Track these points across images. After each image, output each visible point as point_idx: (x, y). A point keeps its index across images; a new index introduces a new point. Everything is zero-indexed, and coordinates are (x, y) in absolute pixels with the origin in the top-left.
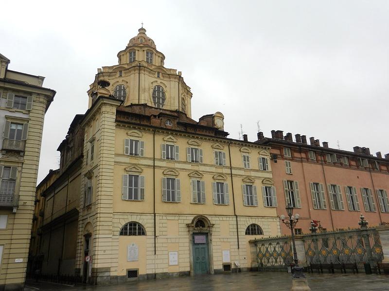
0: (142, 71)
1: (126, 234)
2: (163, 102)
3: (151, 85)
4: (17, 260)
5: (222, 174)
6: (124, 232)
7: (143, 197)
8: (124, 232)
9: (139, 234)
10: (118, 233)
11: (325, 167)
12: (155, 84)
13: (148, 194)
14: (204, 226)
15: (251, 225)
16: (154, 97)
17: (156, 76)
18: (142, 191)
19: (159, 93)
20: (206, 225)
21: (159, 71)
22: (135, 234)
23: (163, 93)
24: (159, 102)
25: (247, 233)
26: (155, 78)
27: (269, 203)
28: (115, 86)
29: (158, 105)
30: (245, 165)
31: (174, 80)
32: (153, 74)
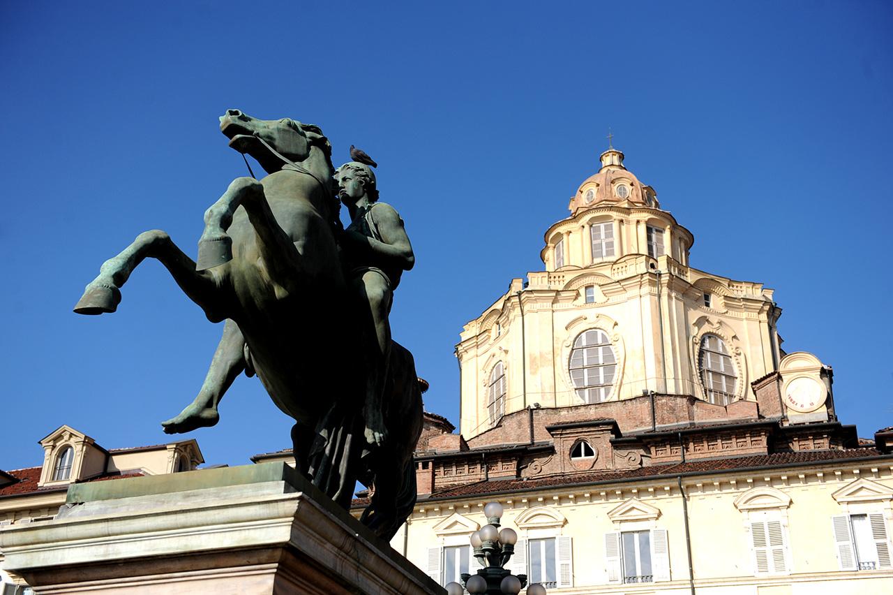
2: (609, 377)
12: (574, 331)
17: (582, 300)
19: (590, 357)
21: (588, 281)
23: (606, 345)
24: (594, 387)
26: (579, 307)
30: (762, 563)
31: (635, 291)
32: (567, 299)
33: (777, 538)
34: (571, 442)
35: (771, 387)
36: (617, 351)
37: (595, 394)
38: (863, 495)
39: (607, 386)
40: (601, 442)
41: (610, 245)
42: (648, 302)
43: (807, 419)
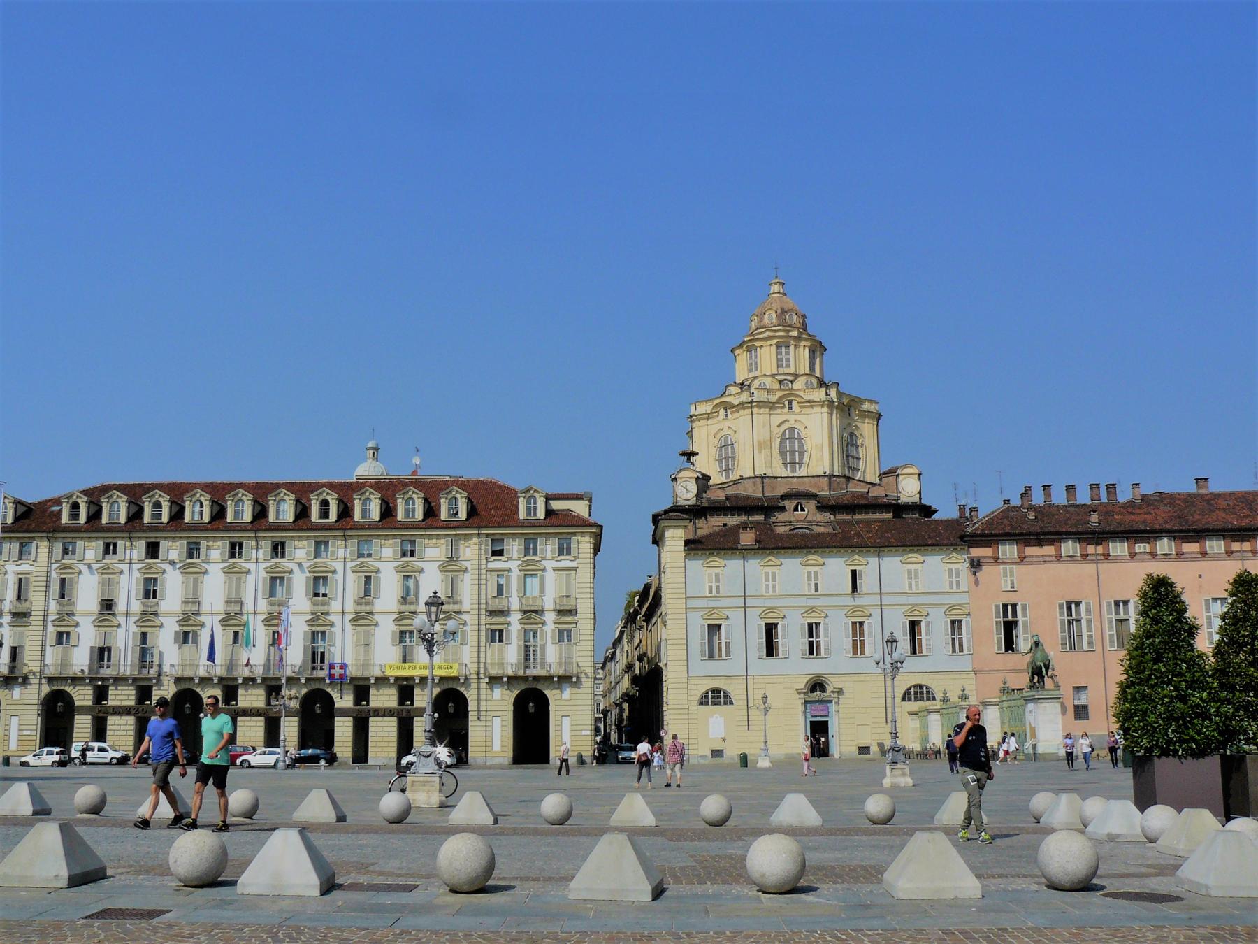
0: (755, 410)
1: (707, 703)
2: (801, 459)
3: (776, 430)
4: (584, 733)
5: (862, 606)
6: (703, 701)
7: (728, 653)
8: (703, 701)
9: (725, 703)
10: (696, 703)
11: (1104, 566)
13: (738, 650)
14: (823, 689)
15: (915, 686)
16: (782, 453)
18: (728, 645)
20: (829, 689)
22: (719, 703)
23: (800, 440)
24: (793, 463)
25: (906, 697)
27: (957, 646)
28: (718, 437)
29: (793, 470)
30: (910, 587)
33: (917, 576)
34: (794, 504)
35: (891, 479)
36: (807, 444)
37: (793, 470)
38: (953, 560)
39: (800, 464)
40: (810, 506)
41: (788, 360)
42: (826, 415)
43: (910, 500)
